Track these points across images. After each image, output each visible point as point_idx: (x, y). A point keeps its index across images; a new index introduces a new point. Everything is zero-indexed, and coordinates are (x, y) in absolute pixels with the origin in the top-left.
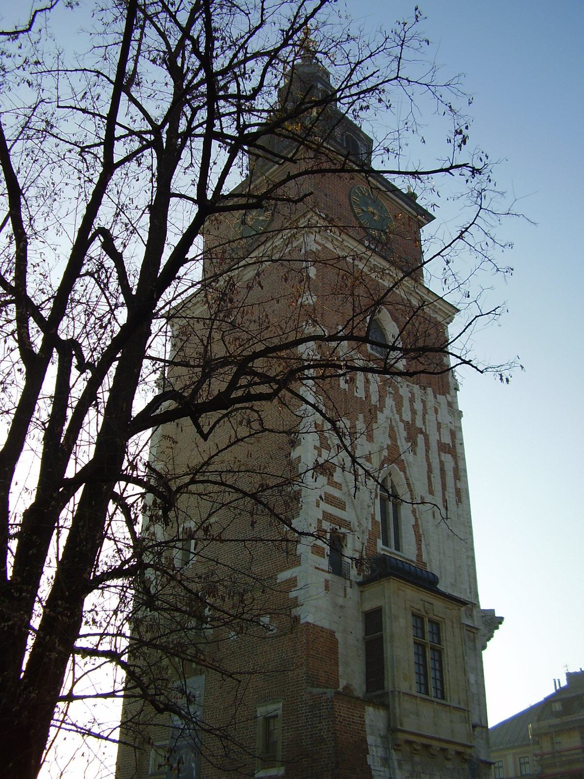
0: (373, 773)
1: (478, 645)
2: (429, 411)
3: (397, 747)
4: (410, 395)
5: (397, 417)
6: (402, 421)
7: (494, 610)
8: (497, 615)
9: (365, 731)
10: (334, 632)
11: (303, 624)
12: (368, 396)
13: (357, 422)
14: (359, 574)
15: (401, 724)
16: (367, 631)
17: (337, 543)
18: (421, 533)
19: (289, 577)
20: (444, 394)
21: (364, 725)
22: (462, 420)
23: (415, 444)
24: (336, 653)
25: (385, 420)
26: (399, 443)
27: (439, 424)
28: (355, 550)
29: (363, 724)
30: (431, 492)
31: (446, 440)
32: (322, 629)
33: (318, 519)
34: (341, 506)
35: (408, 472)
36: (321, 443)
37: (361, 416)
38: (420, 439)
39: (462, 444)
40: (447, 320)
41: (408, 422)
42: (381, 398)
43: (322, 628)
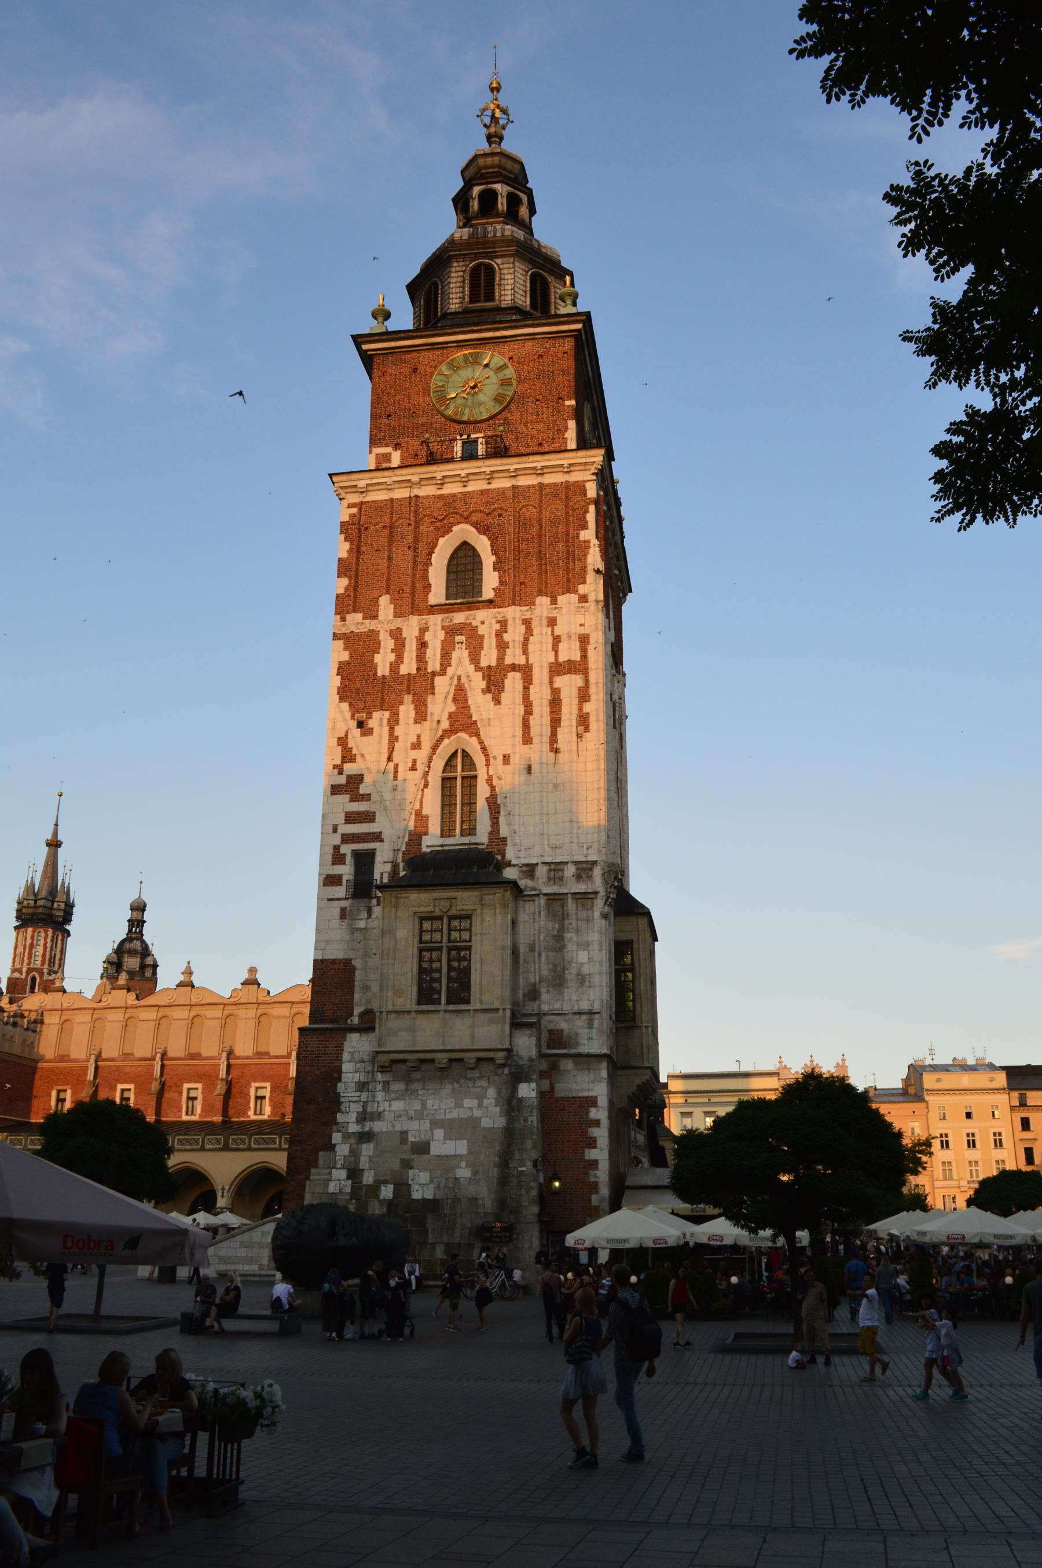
0: (342, 1100)
2: (536, 631)
3: (383, 1069)
4: (498, 627)
6: (478, 668)
10: (350, 960)
17: (364, 861)
20: (569, 591)
26: (470, 702)
27: (557, 640)
30: (527, 740)
32: (333, 961)
34: (369, 817)
36: (343, 758)
37: (408, 698)
40: (593, 470)
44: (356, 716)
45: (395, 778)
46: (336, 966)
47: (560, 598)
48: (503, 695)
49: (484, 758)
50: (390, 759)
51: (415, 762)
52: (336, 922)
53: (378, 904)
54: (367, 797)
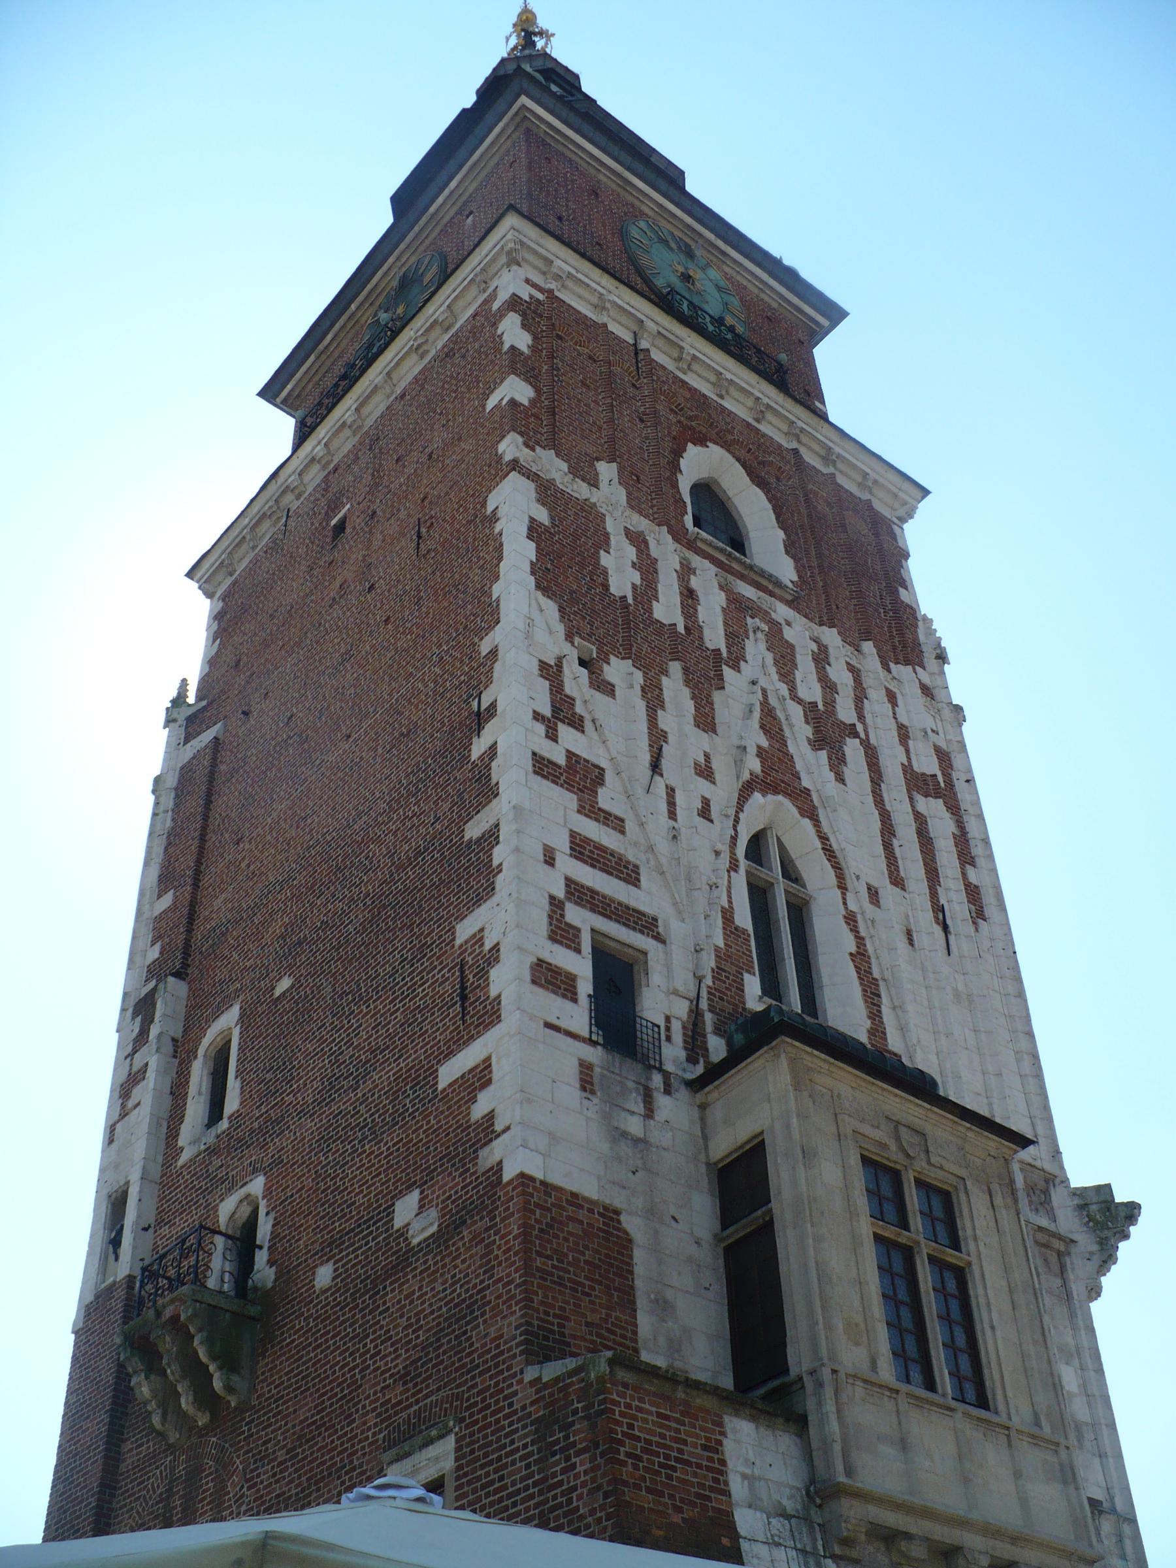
1: (1078, 1289)
2: (871, 693)
4: (814, 647)
5: (784, 689)
7: (1108, 1187)
8: (1119, 1198)
9: (727, 1493)
10: (617, 1212)
11: (512, 1181)
12: (693, 627)
13: (664, 680)
14: (692, 1060)
15: (849, 1472)
16: (727, 1217)
18: (876, 973)
19: (470, 1065)
20: (907, 662)
21: (722, 1473)
22: (966, 728)
23: (837, 763)
24: (626, 1271)
25: (745, 687)
26: (791, 748)
28: (676, 993)
29: (719, 1469)
30: (897, 881)
31: (927, 764)
33: (552, 898)
35: (822, 818)
36: (556, 709)
38: (853, 749)
39: (970, 781)
40: (901, 512)
41: (814, 705)
42: (735, 638)
43: (574, 1195)
44: (577, 640)
45: (672, 815)
46: (582, 1214)
47: (892, 665)
48: (848, 772)
49: (831, 873)
50: (656, 767)
51: (706, 803)
52: (570, 1092)
53: (668, 1091)
54: (616, 823)
